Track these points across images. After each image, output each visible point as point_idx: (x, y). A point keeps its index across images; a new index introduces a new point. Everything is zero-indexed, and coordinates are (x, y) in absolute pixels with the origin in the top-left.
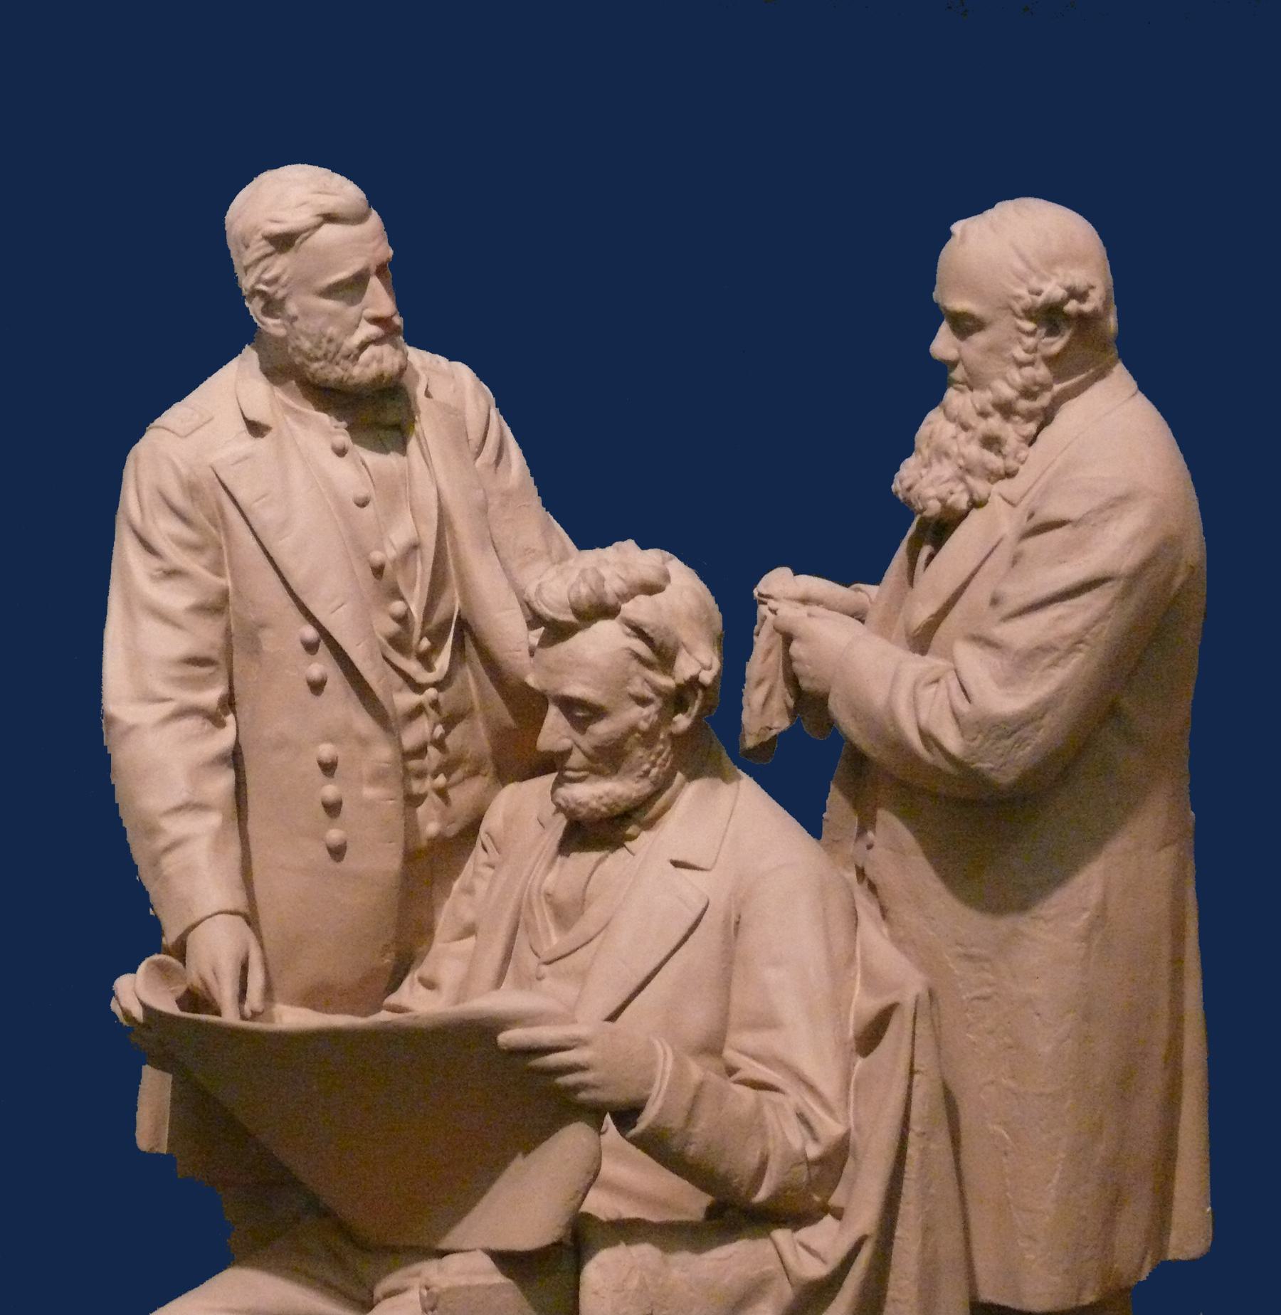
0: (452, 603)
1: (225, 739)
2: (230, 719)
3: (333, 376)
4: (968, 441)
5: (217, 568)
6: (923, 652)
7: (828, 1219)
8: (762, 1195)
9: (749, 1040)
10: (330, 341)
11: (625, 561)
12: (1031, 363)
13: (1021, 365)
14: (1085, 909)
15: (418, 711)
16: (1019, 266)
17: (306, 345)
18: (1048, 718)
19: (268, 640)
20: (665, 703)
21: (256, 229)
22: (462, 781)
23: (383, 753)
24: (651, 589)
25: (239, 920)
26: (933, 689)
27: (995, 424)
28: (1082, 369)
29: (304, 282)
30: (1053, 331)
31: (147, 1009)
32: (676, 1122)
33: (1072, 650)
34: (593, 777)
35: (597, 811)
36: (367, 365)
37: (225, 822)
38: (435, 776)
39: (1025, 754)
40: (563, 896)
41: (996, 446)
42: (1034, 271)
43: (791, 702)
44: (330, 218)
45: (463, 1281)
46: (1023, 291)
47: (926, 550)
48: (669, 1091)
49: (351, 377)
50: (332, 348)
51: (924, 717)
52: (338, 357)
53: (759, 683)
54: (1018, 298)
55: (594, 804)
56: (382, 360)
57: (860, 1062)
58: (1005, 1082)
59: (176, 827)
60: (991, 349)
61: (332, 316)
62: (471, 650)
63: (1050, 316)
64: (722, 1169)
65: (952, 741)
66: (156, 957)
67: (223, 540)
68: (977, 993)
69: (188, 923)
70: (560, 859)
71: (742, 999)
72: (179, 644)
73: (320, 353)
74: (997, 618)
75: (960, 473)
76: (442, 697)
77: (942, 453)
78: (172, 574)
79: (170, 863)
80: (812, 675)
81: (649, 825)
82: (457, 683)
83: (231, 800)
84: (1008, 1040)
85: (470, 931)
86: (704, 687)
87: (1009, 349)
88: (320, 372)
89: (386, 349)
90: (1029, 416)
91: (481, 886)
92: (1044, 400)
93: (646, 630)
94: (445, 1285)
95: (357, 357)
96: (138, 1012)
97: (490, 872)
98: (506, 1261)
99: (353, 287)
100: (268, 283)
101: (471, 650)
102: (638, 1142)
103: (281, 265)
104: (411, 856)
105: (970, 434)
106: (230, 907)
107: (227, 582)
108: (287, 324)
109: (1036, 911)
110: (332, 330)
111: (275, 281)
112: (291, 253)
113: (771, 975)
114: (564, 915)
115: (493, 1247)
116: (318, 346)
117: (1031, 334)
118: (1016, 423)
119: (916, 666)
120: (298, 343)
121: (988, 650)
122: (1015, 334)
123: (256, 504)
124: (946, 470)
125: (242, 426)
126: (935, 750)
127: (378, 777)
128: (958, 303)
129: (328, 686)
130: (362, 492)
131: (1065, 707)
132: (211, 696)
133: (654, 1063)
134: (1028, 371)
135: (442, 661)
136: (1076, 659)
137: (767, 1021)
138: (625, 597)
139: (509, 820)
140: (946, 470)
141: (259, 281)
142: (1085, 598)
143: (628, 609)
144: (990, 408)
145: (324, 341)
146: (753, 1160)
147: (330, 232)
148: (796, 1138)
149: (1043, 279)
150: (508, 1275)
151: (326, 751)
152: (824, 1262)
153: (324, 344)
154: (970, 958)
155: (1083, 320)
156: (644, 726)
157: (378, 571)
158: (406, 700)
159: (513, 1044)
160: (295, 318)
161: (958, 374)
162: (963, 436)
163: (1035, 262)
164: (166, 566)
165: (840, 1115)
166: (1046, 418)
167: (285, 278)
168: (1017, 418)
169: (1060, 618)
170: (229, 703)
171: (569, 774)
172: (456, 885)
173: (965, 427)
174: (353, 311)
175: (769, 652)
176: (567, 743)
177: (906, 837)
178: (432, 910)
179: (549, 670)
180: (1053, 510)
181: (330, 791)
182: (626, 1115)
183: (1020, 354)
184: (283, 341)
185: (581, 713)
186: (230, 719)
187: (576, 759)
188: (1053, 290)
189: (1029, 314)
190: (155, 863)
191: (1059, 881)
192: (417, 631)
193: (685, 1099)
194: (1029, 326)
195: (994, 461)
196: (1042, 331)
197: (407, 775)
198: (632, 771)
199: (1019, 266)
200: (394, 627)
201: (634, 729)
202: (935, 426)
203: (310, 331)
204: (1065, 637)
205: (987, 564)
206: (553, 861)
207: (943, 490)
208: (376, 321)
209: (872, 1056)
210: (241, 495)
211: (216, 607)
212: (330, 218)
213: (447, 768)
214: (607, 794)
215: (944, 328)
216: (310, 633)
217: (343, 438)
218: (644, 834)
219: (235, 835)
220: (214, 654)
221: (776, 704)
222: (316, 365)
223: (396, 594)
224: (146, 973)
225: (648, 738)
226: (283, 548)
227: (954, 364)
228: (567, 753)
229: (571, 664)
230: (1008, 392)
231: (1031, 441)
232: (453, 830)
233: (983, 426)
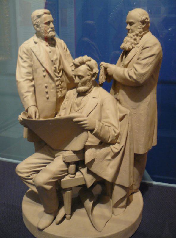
0: (61, 67)
1: (33, 83)
2: (33, 81)
5: (31, 61)
6: (126, 68)
7: (116, 144)
8: (109, 141)
9: (105, 120)
11: (85, 58)
12: (141, 28)
13: (139, 29)
14: (148, 101)
15: (57, 80)
16: (140, 15)
17: (42, 31)
18: (147, 74)
19: (38, 70)
20: (92, 76)
22: (63, 90)
23: (53, 85)
24: (90, 61)
25: (35, 107)
26: (131, 71)
27: (135, 37)
28: (146, 30)
29: (41, 22)
30: (143, 24)
31: (23, 119)
32: (99, 131)
37: (33, 94)
38: (60, 89)
39: (144, 79)
40: (78, 103)
43: (106, 78)
44: (45, 13)
45: (68, 155)
47: (124, 57)
48: (98, 127)
50: (46, 31)
51: (130, 74)
53: (101, 76)
54: (139, 19)
55: (82, 90)
56: (52, 34)
57: (120, 123)
58: (138, 125)
59: (26, 94)
60: (135, 27)
62: (64, 73)
63: (143, 22)
64: (105, 138)
65: (135, 77)
66: (24, 112)
67: (32, 57)
68: (134, 113)
69: (28, 107)
71: (104, 115)
72: (26, 71)
76: (61, 79)
77: (128, 41)
78: (25, 61)
79: (25, 99)
82: (62, 77)
83: (34, 91)
84: (138, 119)
85: (65, 109)
86: (97, 74)
89: (53, 32)
90: (140, 36)
91: (66, 103)
92: (142, 34)
94: (66, 155)
95: (49, 33)
96: (22, 119)
97: (67, 101)
98: (74, 152)
99: (48, 23)
101: (64, 73)
102: (94, 134)
103: (39, 20)
104: (57, 99)
106: (34, 104)
107: (32, 63)
109: (142, 102)
111: (38, 22)
112: (40, 18)
113: (108, 111)
114: (78, 105)
116: (44, 31)
117: (141, 24)
119: (126, 70)
124: (129, 44)
125: (34, 43)
127: (53, 88)
128: (131, 20)
129: (46, 76)
130: (50, 51)
131: (149, 72)
132: (31, 78)
133: (96, 123)
134: (140, 29)
135: (61, 74)
136: (151, 66)
137: (107, 117)
138: (86, 61)
139: (69, 95)
140: (129, 44)
142: (152, 57)
146: (109, 136)
147: (45, 15)
148: (114, 133)
149: (143, 17)
151: (46, 85)
152: (118, 149)
154: (133, 108)
155: (148, 23)
156: (89, 79)
157: (52, 61)
158: (56, 79)
159: (76, 121)
161: (130, 31)
162: (131, 39)
164: (24, 60)
166: (142, 36)
169: (149, 60)
170: (33, 79)
172: (63, 103)
173: (131, 38)
174: (48, 27)
175: (103, 71)
176: (78, 82)
177: (124, 93)
178: (60, 106)
180: (147, 45)
181: (47, 90)
182: (92, 131)
185: (80, 77)
186: (33, 81)
187: (80, 84)
188: (144, 18)
190: (23, 99)
191: (145, 97)
192: (57, 70)
193: (100, 128)
194: (140, 23)
195: (136, 42)
196: (142, 24)
197: (57, 89)
198: (87, 85)
199: (140, 15)
200: (54, 69)
201: (87, 79)
202: (126, 38)
206: (76, 99)
207: (129, 46)
208: (52, 28)
209: (121, 122)
210: (34, 51)
211: (31, 66)
212: (45, 13)
213: (62, 88)
216: (43, 69)
217: (47, 44)
218: (89, 94)
219: (34, 95)
220: (31, 72)
221: (104, 78)
223: (54, 64)
224: (23, 114)
225: (89, 81)
226: (40, 58)
227: (129, 30)
228: (78, 83)
230: (137, 33)
231: (140, 39)
232: (62, 96)
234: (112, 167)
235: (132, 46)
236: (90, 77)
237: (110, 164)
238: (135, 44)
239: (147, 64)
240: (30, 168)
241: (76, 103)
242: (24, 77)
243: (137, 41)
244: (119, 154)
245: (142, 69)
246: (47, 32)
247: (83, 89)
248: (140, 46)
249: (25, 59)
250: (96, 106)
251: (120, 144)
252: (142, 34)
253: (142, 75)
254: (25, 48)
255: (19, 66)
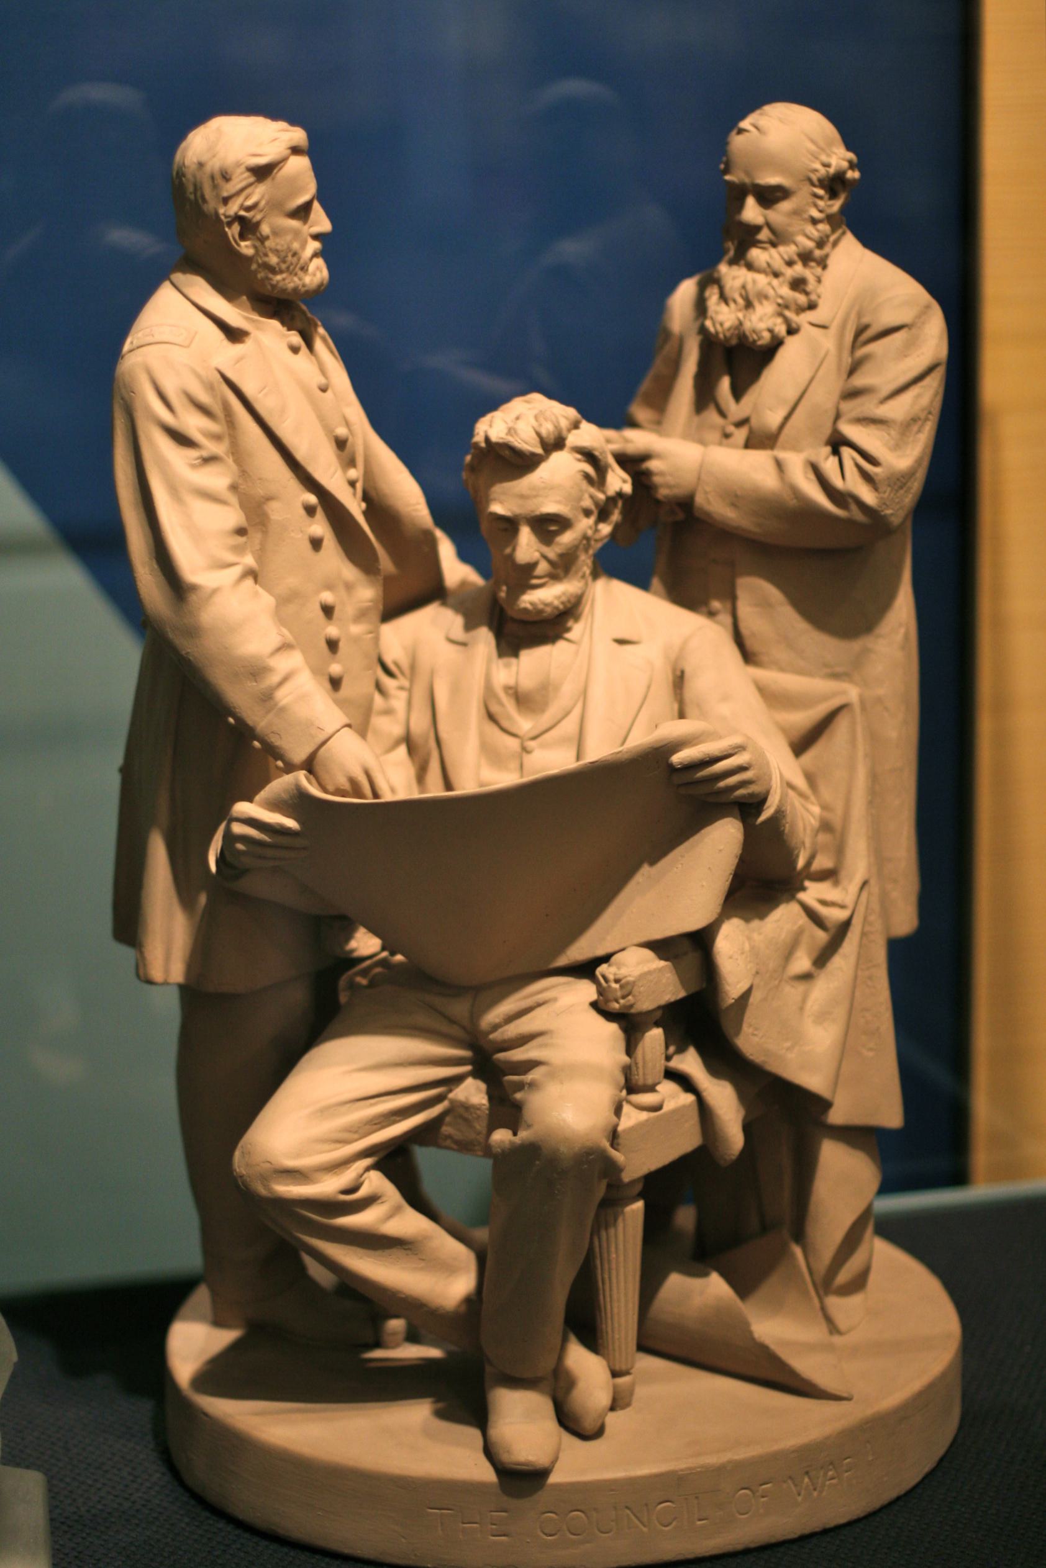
3: (291, 286)
4: (781, 285)
10: (295, 254)
13: (814, 222)
16: (813, 147)
17: (273, 260)
19: (276, 512)
21: (238, 164)
27: (798, 269)
29: (275, 205)
30: (833, 194)
33: (927, 419)
34: (552, 582)
35: (557, 608)
36: (314, 275)
40: (527, 683)
41: (802, 286)
42: (823, 150)
46: (818, 166)
49: (304, 286)
51: (837, 482)
52: (297, 269)
54: (816, 170)
55: (556, 603)
59: (283, 664)
60: (796, 213)
61: (297, 233)
63: (834, 184)
65: (868, 496)
70: (501, 662)
73: (284, 266)
74: (875, 401)
75: (779, 309)
79: (284, 696)
80: (672, 483)
81: (577, 619)
87: (806, 211)
88: (281, 284)
93: (597, 453)
99: (303, 212)
100: (248, 209)
103: (258, 193)
105: (781, 279)
108: (258, 244)
110: (296, 246)
115: (658, 935)
117: (820, 198)
118: (812, 268)
120: (266, 259)
121: (879, 426)
122: (811, 199)
123: (260, 395)
126: (854, 507)
128: (772, 179)
129: (325, 543)
131: (926, 463)
134: (821, 226)
141: (242, 207)
142: (928, 381)
143: (573, 439)
144: (796, 258)
145: (290, 255)
150: (666, 960)
151: (327, 597)
153: (289, 258)
160: (267, 238)
161: (764, 235)
162: (775, 282)
163: (822, 144)
164: (205, 454)
165: (812, 798)
166: (823, 263)
167: (263, 203)
168: (813, 264)
169: (919, 396)
171: (535, 582)
173: (776, 275)
176: (537, 555)
177: (772, 592)
179: (522, 497)
181: (332, 631)
183: (815, 214)
184: (249, 260)
185: (547, 526)
187: (543, 567)
189: (822, 183)
190: (267, 698)
194: (821, 192)
195: (802, 299)
196: (827, 197)
198: (576, 572)
203: (279, 247)
204: (923, 410)
205: (821, 373)
207: (769, 323)
210: (249, 389)
212: (296, 150)
214: (564, 594)
215: (750, 201)
216: (312, 499)
217: (295, 338)
222: (279, 277)
227: (757, 229)
228: (533, 566)
229: (545, 488)
230: (810, 244)
231: (819, 281)
233: (790, 273)
234: (822, 1017)
235: (787, 321)
236: (591, 521)
237: (809, 1003)
238: (800, 310)
239: (914, 420)
240: (346, 1136)
241: (507, 688)
242: (230, 557)
243: (807, 293)
244: (849, 935)
245: (897, 447)
246: (299, 260)
247: (558, 598)
248: (834, 318)
249: (212, 448)
250: (649, 687)
251: (843, 874)
252: (827, 249)
253: (900, 480)
254: (198, 376)
255: (174, 490)
